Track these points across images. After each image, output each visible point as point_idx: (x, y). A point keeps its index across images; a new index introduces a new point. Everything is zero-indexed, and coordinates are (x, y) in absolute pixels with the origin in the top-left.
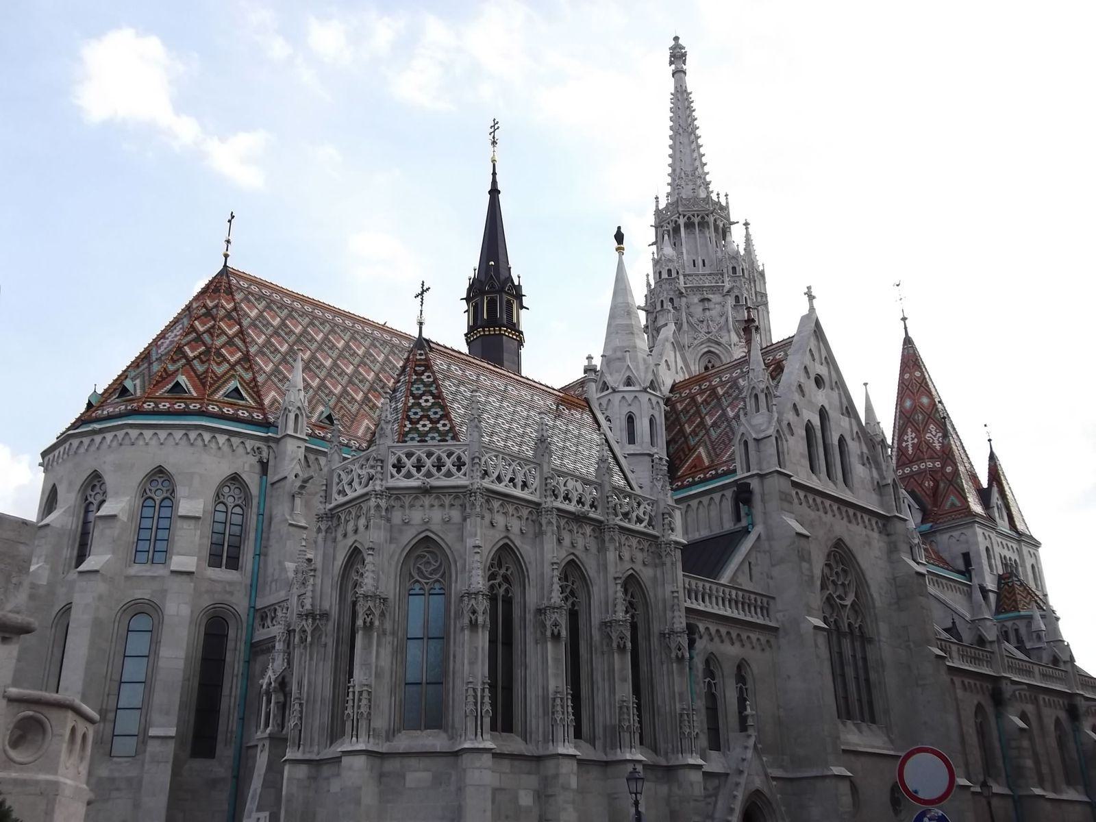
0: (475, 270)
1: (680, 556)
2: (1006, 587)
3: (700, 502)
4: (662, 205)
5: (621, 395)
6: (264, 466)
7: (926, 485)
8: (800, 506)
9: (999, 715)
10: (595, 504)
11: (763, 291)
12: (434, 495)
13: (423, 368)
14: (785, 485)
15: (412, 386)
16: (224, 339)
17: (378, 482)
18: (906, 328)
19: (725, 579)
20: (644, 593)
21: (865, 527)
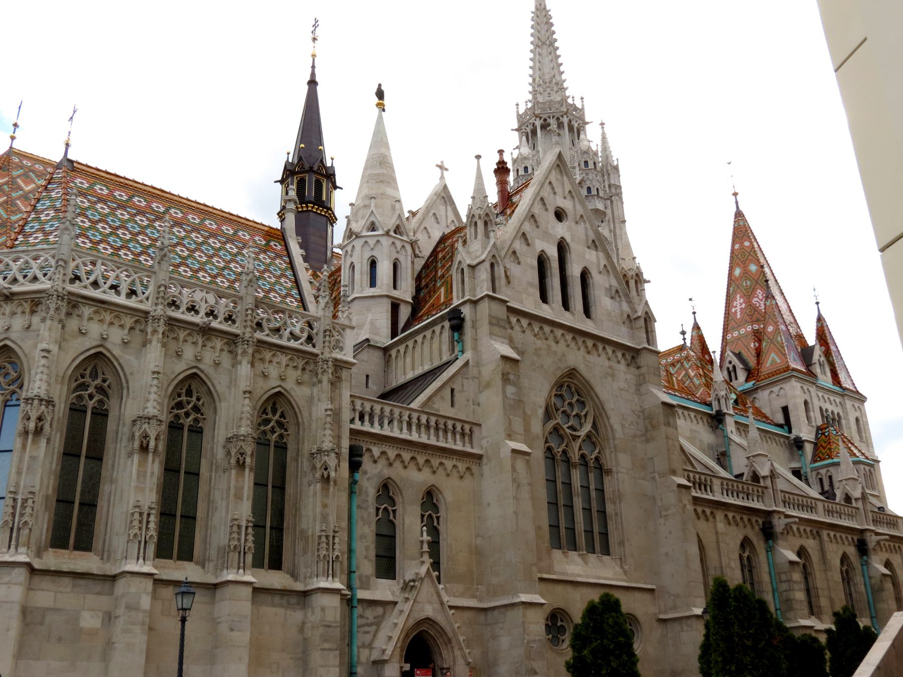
0: (288, 154)
2: (823, 436)
3: (425, 336)
4: (522, 111)
5: (363, 240)
7: (752, 345)
9: (770, 550)
11: (617, 184)
12: (16, 301)
18: (737, 203)
20: (295, 413)
21: (609, 359)
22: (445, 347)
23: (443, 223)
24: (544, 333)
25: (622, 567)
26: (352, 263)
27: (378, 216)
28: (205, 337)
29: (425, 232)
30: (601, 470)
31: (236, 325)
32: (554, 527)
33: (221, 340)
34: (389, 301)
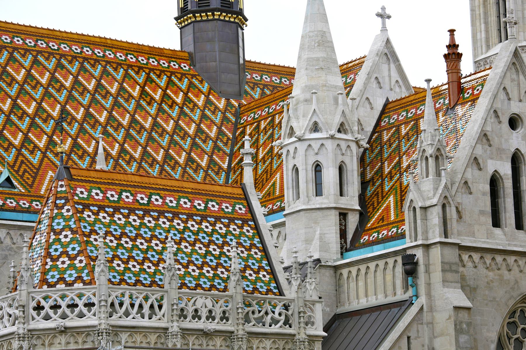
1: (321, 347)
5: (307, 143)
8: (474, 269)
10: (227, 315)
12: (70, 334)
13: (63, 201)
14: (452, 254)
15: (53, 222)
17: (21, 326)
22: (399, 282)
23: (387, 87)
24: (496, 264)
26: (295, 165)
27: (320, 116)
28: (207, 339)
29: (367, 102)
31: (230, 322)
33: (220, 338)
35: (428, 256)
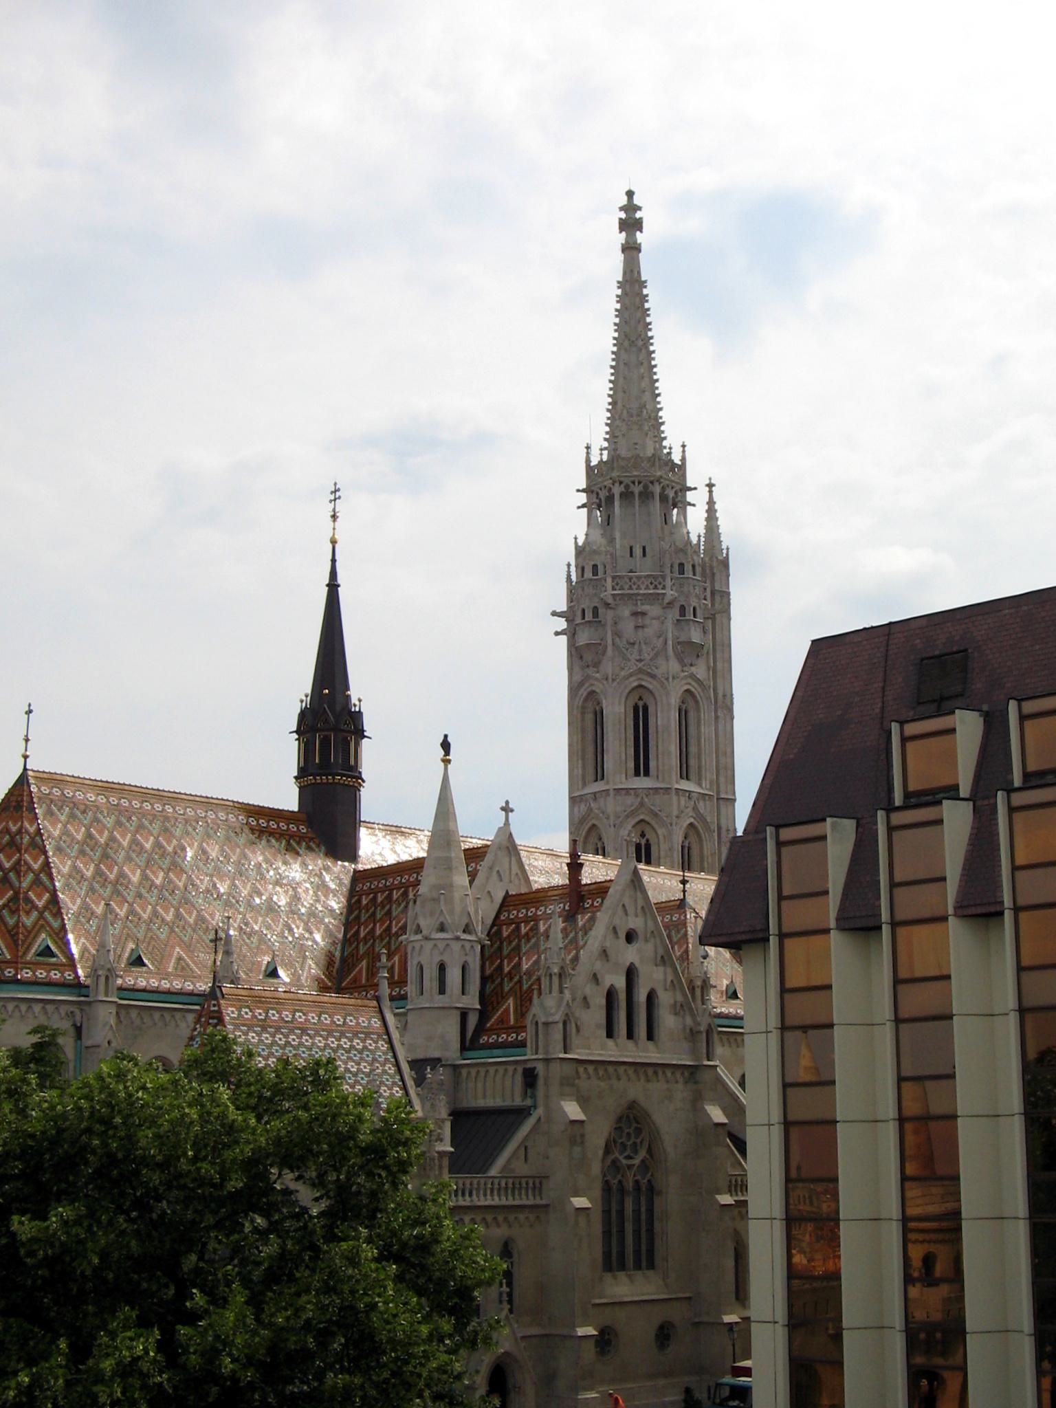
4: (594, 462)
5: (433, 942)
6: (78, 1030)
13: (215, 1021)
14: (568, 1069)
16: (31, 876)
19: (494, 1172)
25: (664, 1280)
27: (447, 917)
30: (652, 1190)
32: (607, 1255)
34: (458, 1013)
35: (548, 1069)
